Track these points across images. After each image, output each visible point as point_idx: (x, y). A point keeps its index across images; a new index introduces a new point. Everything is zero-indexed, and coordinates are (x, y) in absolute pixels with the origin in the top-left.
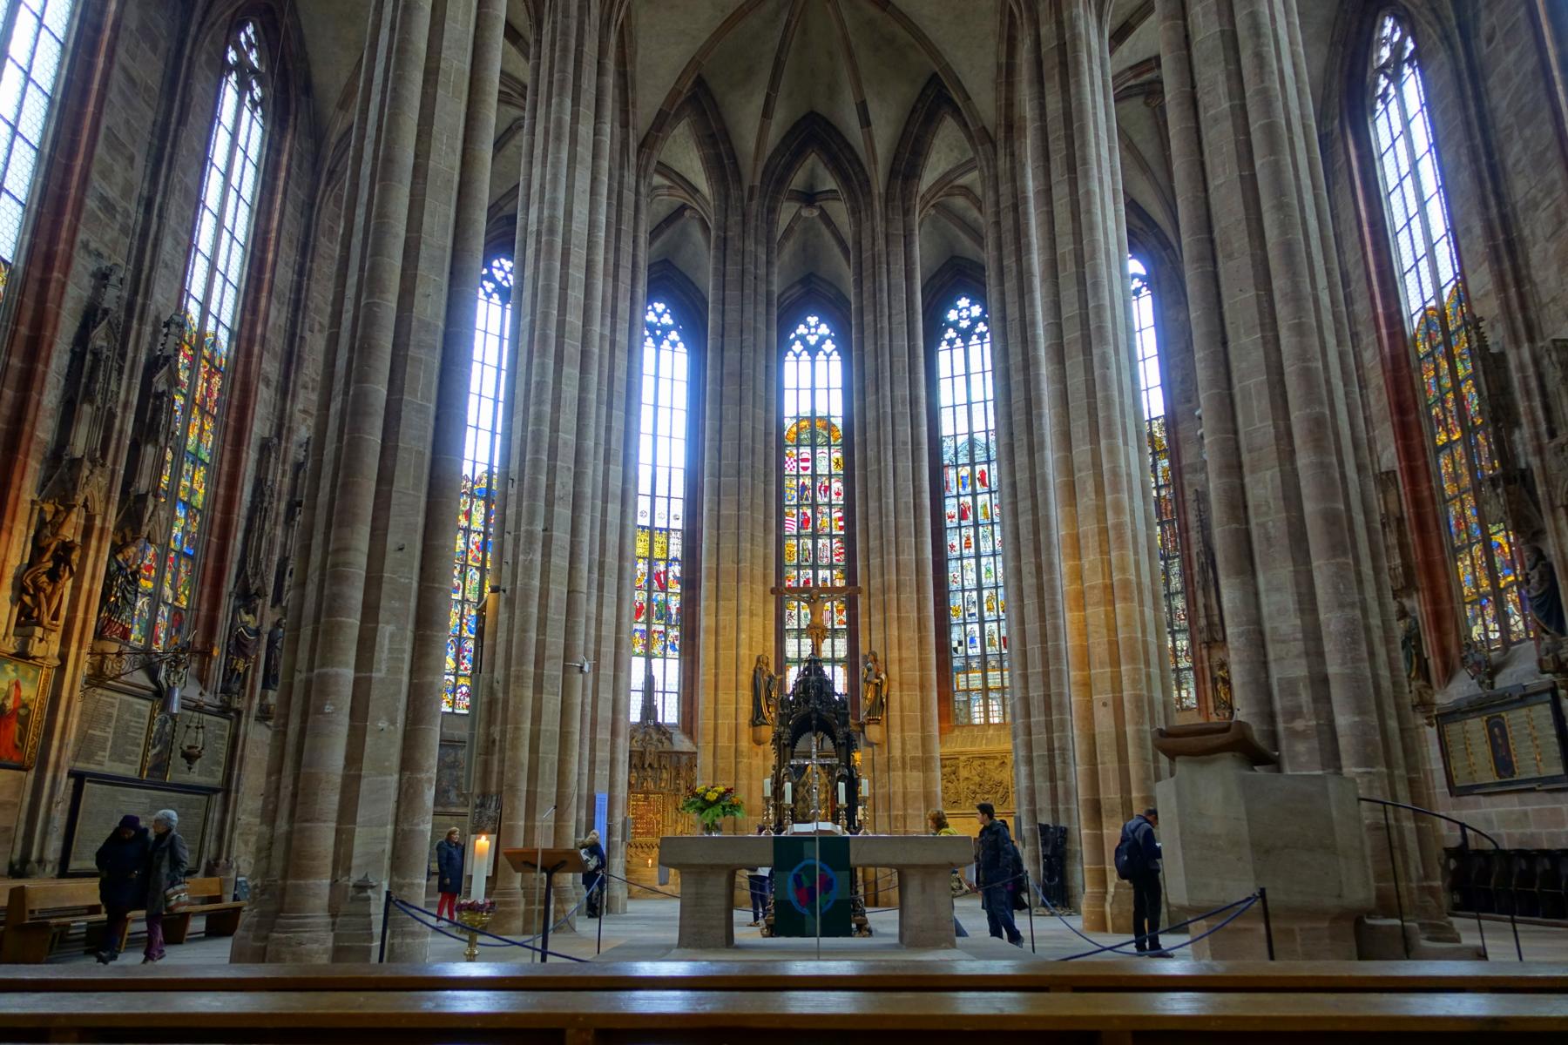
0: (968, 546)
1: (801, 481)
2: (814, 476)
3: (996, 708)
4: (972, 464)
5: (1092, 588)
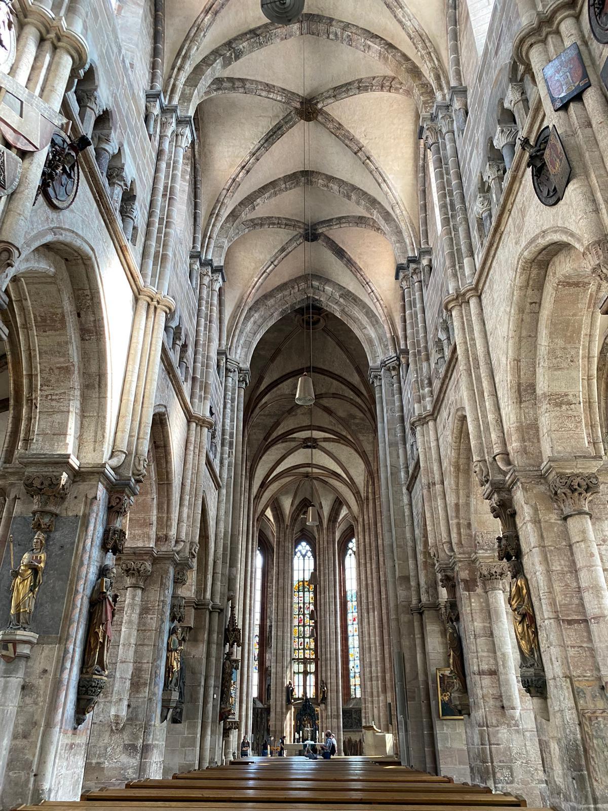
2: (304, 603)
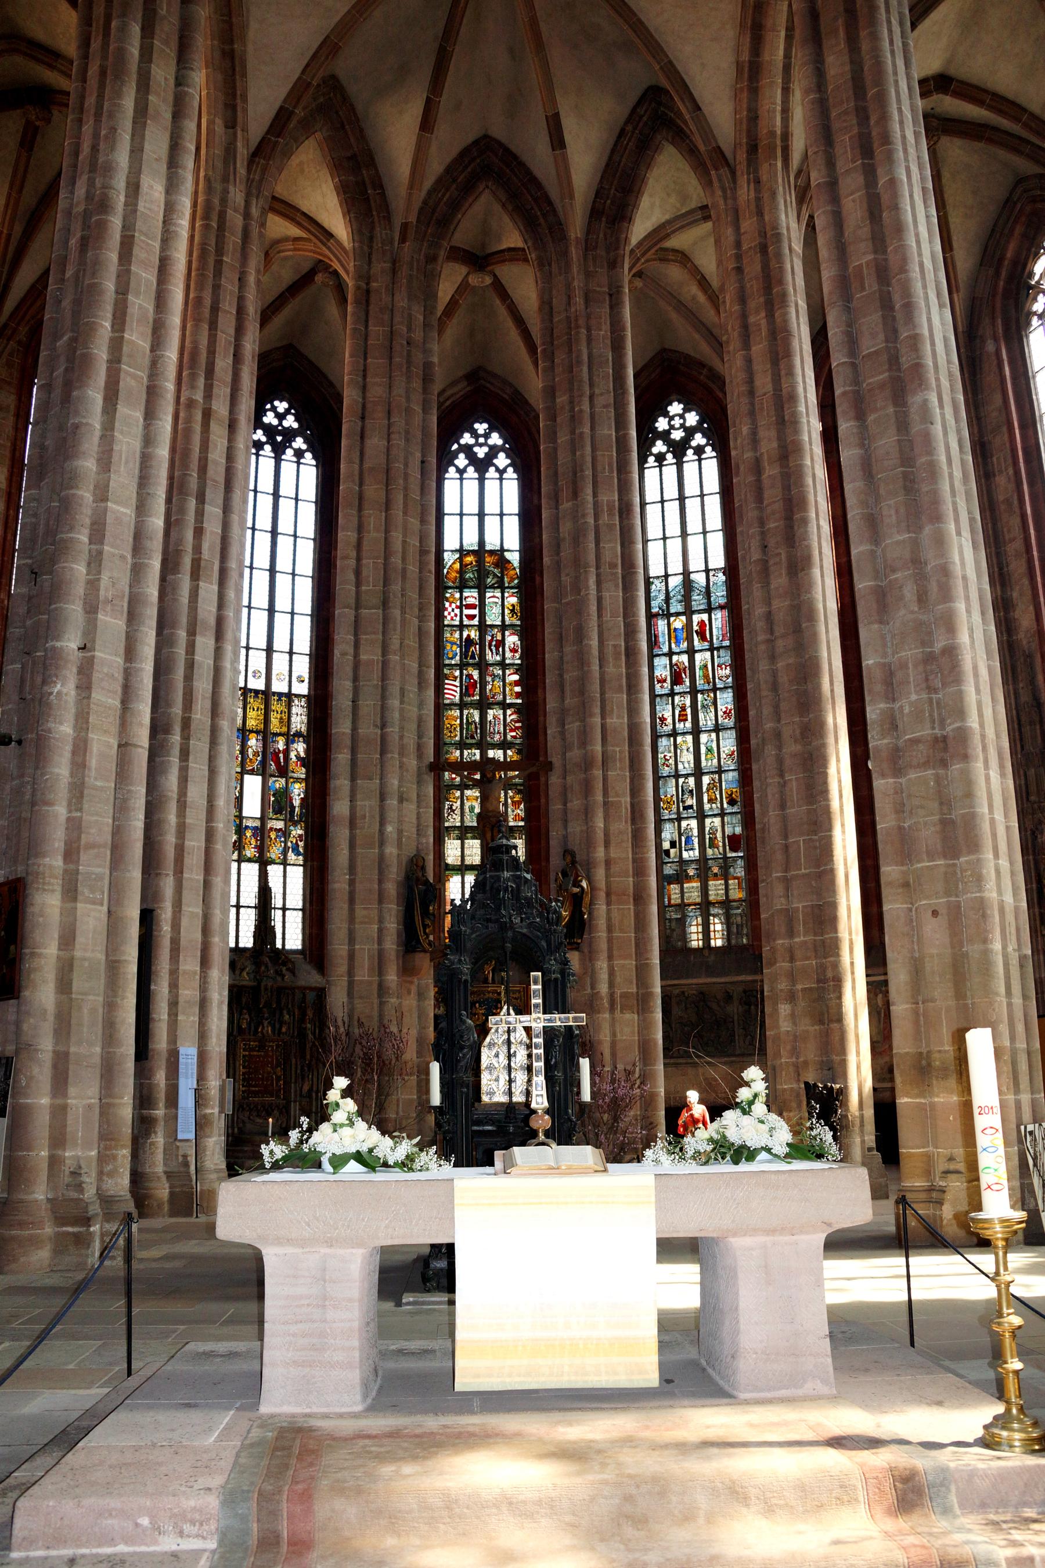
0: (683, 718)
1: (465, 634)
2: (483, 627)
3: (719, 927)
4: (689, 612)
5: (916, 741)
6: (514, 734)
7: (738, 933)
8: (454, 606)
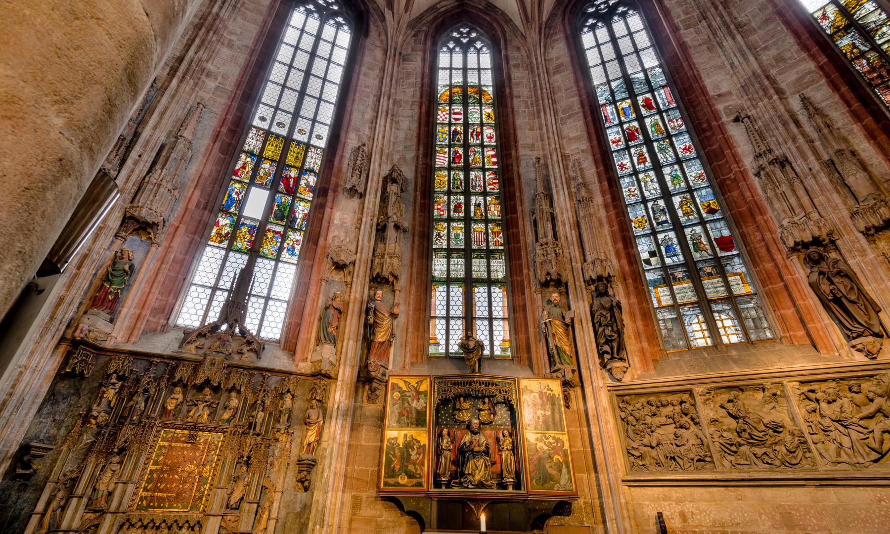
1: (453, 128)
2: (466, 125)
3: (728, 323)
6: (492, 187)
7: (756, 327)
8: (444, 113)
